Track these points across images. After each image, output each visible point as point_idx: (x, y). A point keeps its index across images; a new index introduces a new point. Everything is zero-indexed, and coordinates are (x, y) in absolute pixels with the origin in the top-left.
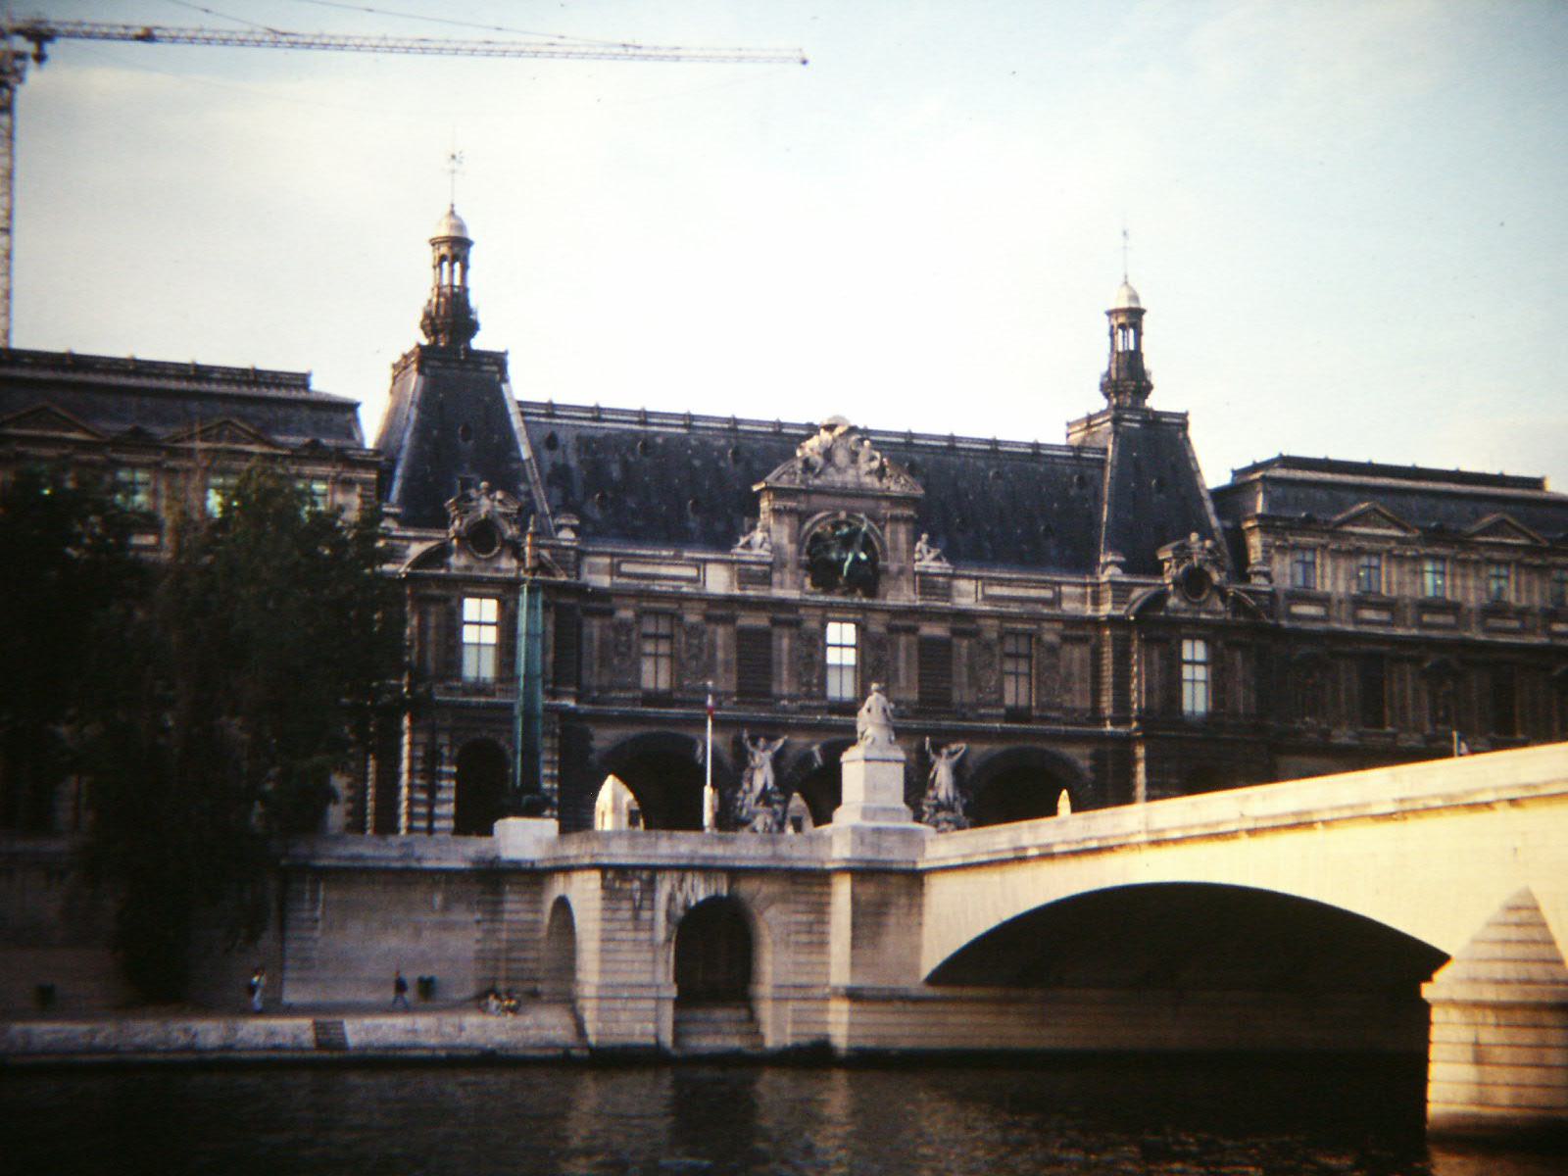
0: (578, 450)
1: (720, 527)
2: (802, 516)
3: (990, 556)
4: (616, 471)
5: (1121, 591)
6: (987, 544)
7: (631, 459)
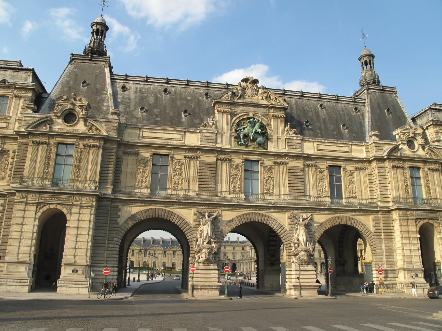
0: (136, 92)
1: (197, 121)
2: (232, 115)
3: (319, 135)
4: (151, 100)
5: (379, 147)
6: (319, 132)
7: (159, 96)
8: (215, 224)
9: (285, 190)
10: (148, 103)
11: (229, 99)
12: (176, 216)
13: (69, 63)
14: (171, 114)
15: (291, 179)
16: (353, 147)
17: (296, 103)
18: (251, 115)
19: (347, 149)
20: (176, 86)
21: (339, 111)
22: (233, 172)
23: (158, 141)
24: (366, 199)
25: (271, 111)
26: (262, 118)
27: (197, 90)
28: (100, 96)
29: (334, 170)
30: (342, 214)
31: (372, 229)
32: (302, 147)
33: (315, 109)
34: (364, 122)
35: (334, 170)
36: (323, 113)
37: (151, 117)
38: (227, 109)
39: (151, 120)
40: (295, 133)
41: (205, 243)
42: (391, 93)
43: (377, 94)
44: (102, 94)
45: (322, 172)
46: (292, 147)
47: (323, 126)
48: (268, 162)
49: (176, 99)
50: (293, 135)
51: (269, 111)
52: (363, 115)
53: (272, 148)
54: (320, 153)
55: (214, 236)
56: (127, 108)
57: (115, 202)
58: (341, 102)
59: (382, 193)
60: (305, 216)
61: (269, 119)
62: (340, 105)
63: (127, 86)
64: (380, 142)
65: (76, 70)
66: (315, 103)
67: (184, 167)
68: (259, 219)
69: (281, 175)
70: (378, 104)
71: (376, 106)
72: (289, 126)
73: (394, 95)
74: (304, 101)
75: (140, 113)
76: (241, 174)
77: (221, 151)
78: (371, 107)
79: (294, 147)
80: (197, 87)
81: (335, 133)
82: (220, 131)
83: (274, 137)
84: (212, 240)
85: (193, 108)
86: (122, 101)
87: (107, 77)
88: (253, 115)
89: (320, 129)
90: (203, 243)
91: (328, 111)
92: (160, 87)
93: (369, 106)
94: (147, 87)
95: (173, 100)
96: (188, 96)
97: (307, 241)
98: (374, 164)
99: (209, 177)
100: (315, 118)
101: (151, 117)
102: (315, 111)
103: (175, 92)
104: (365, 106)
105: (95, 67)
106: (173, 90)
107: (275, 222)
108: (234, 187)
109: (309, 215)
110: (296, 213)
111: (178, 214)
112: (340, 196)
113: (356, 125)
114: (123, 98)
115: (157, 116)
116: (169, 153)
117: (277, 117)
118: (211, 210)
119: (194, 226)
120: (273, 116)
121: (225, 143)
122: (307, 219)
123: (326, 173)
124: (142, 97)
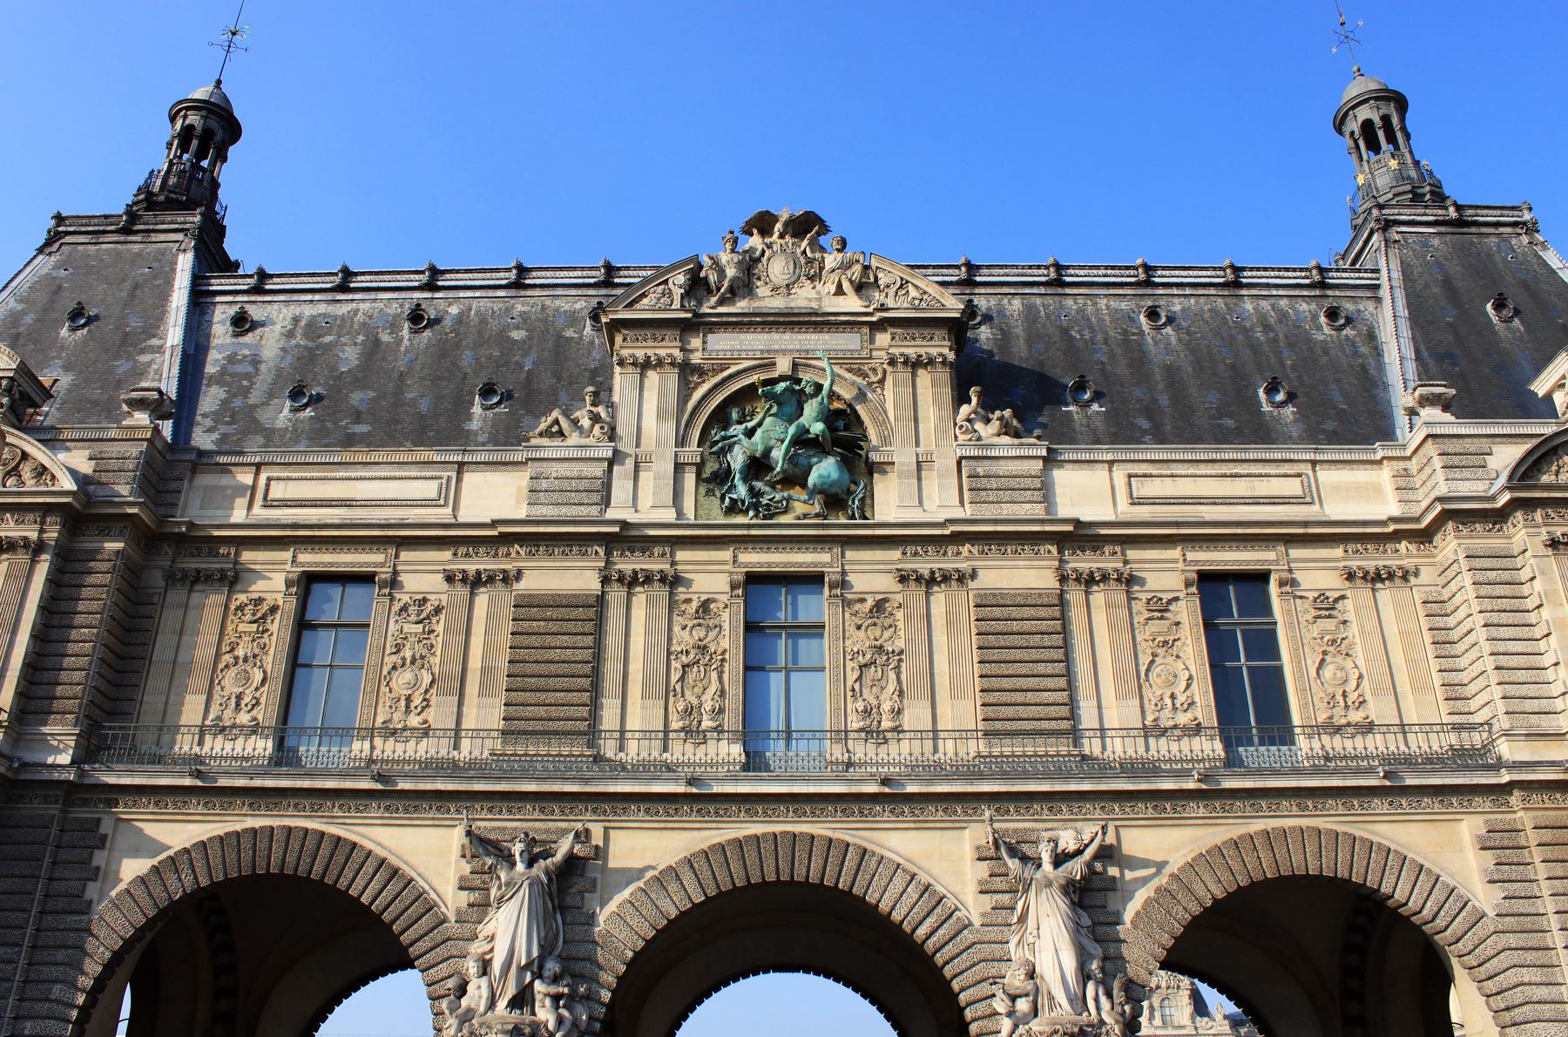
0: (290, 334)
4: (350, 356)
7: (385, 337)
8: (569, 901)
9: (960, 711)
10: (333, 368)
11: (677, 304)
12: (369, 867)
13: (40, 251)
14: (424, 406)
15: (995, 655)
16: (1326, 476)
17: (1030, 313)
19: (1292, 487)
20: (469, 294)
21: (1245, 330)
22: (684, 638)
24: (1426, 728)
25: (883, 339)
26: (833, 374)
27: (557, 303)
28: (130, 357)
29: (1233, 602)
30: (1289, 820)
31: (1486, 898)
32: (1046, 492)
33: (1125, 332)
34: (1381, 367)
35: (1233, 602)
36: (1162, 343)
37: (329, 425)
38: (669, 349)
40: (1006, 430)
41: (502, 1004)
42: (1509, 230)
43: (1436, 242)
44: (143, 351)
45: (1160, 608)
46: (992, 496)
47: (1164, 400)
48: (871, 574)
49: (458, 345)
50: (996, 440)
51: (872, 341)
52: (1371, 337)
53: (891, 502)
54: (1144, 513)
55: (552, 966)
56: (235, 396)
57: (85, 803)
58: (1254, 292)
59: (1513, 690)
60: (1068, 841)
61: (874, 379)
62: (1249, 306)
63: (255, 312)
64: (1463, 431)
66: (1124, 305)
67: (440, 628)
68: (811, 869)
69: (940, 638)
70: (1447, 283)
71: (1436, 290)
72: (974, 400)
73: (1525, 239)
74: (1069, 302)
75: (286, 411)
76: (725, 644)
77: (626, 538)
78: (1407, 296)
79: (1007, 495)
80: (560, 292)
81: (1229, 422)
82: (626, 446)
83: (903, 456)
84: (539, 986)
85: (529, 372)
86: (223, 372)
87: (177, 286)
88: (795, 366)
89: (1150, 412)
90: (492, 1004)
91: (1188, 333)
92: (395, 305)
93: (1400, 294)
94: (343, 310)
95: (444, 352)
96: (518, 328)
97: (1084, 976)
98: (1450, 544)
99: (560, 664)
100: (1122, 369)
101: (329, 425)
102: (1126, 341)
103: (460, 319)
104: (1378, 300)
105: (139, 254)
107: (899, 882)
108: (688, 711)
109: (1089, 830)
110: (1015, 824)
111: (383, 853)
112: (1277, 726)
113: (1338, 381)
114: (231, 359)
115: (358, 417)
116: (376, 565)
117: (915, 365)
118: (535, 823)
119: (458, 912)
120: (892, 362)
121: (646, 500)
122: (1079, 852)
123: (1188, 612)
124: (310, 350)
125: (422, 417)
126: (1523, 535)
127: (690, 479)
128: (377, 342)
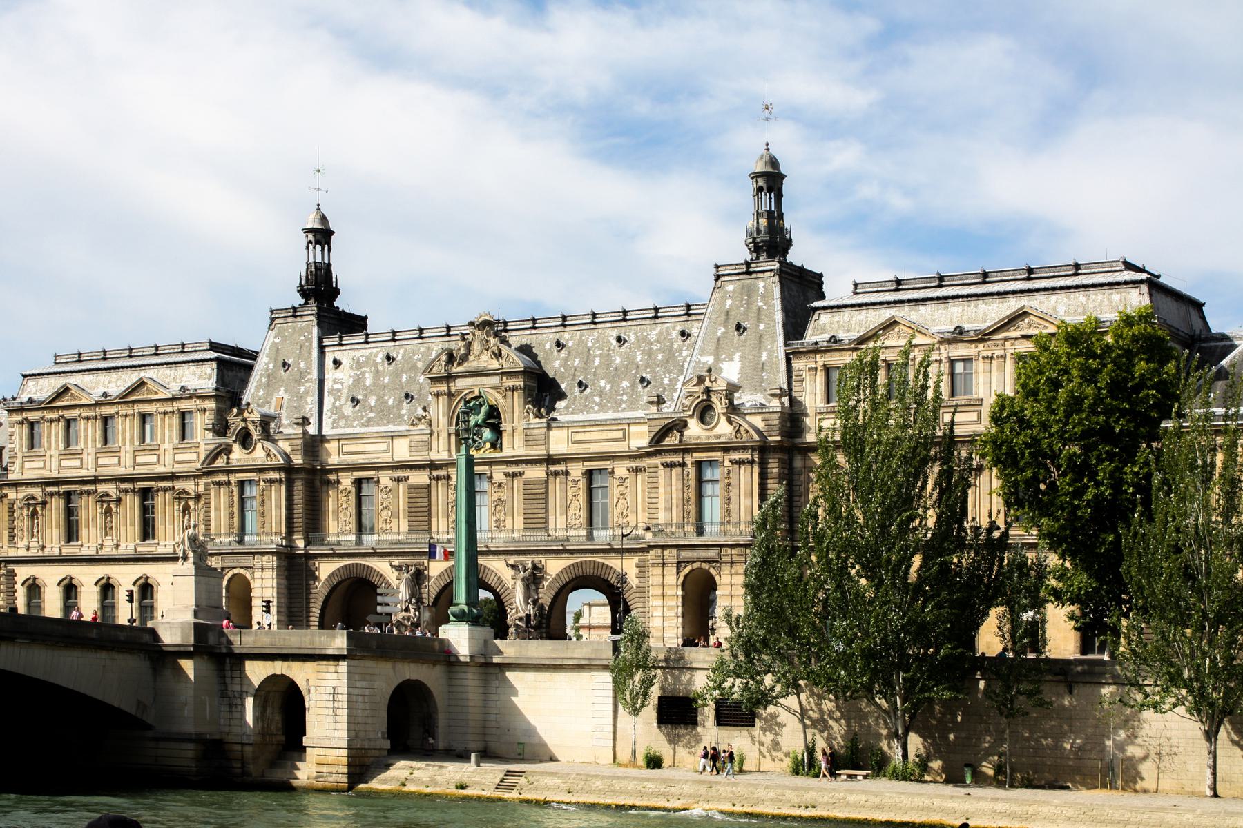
3: (596, 408)
6: (597, 399)
7: (380, 368)
14: (391, 402)
18: (477, 393)
23: (360, 459)
39: (362, 417)
45: (576, 482)
47: (608, 387)
54: (575, 449)
65: (277, 341)
106: (401, 351)
125: (389, 408)
126: (658, 460)
127: (453, 438)
128: (378, 371)
